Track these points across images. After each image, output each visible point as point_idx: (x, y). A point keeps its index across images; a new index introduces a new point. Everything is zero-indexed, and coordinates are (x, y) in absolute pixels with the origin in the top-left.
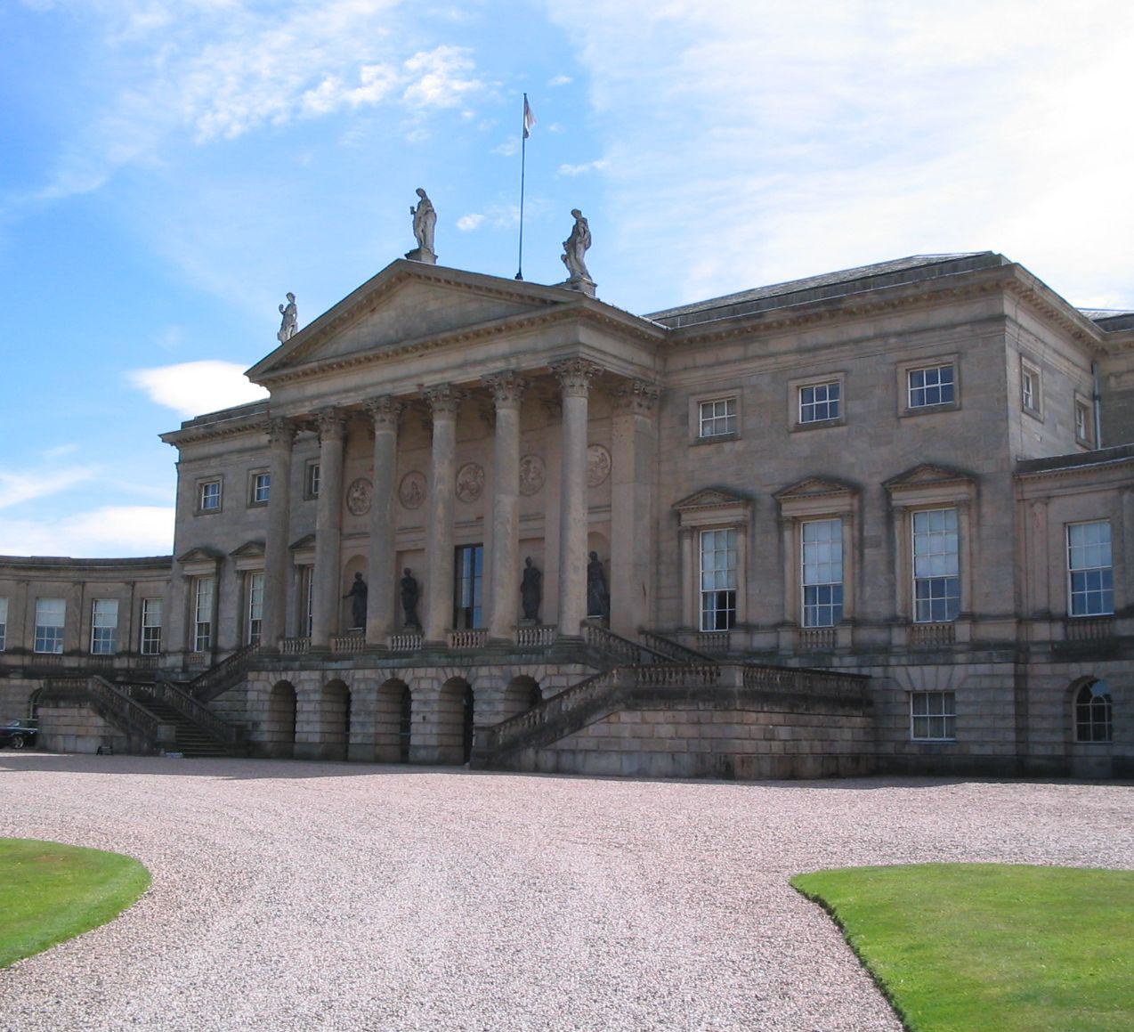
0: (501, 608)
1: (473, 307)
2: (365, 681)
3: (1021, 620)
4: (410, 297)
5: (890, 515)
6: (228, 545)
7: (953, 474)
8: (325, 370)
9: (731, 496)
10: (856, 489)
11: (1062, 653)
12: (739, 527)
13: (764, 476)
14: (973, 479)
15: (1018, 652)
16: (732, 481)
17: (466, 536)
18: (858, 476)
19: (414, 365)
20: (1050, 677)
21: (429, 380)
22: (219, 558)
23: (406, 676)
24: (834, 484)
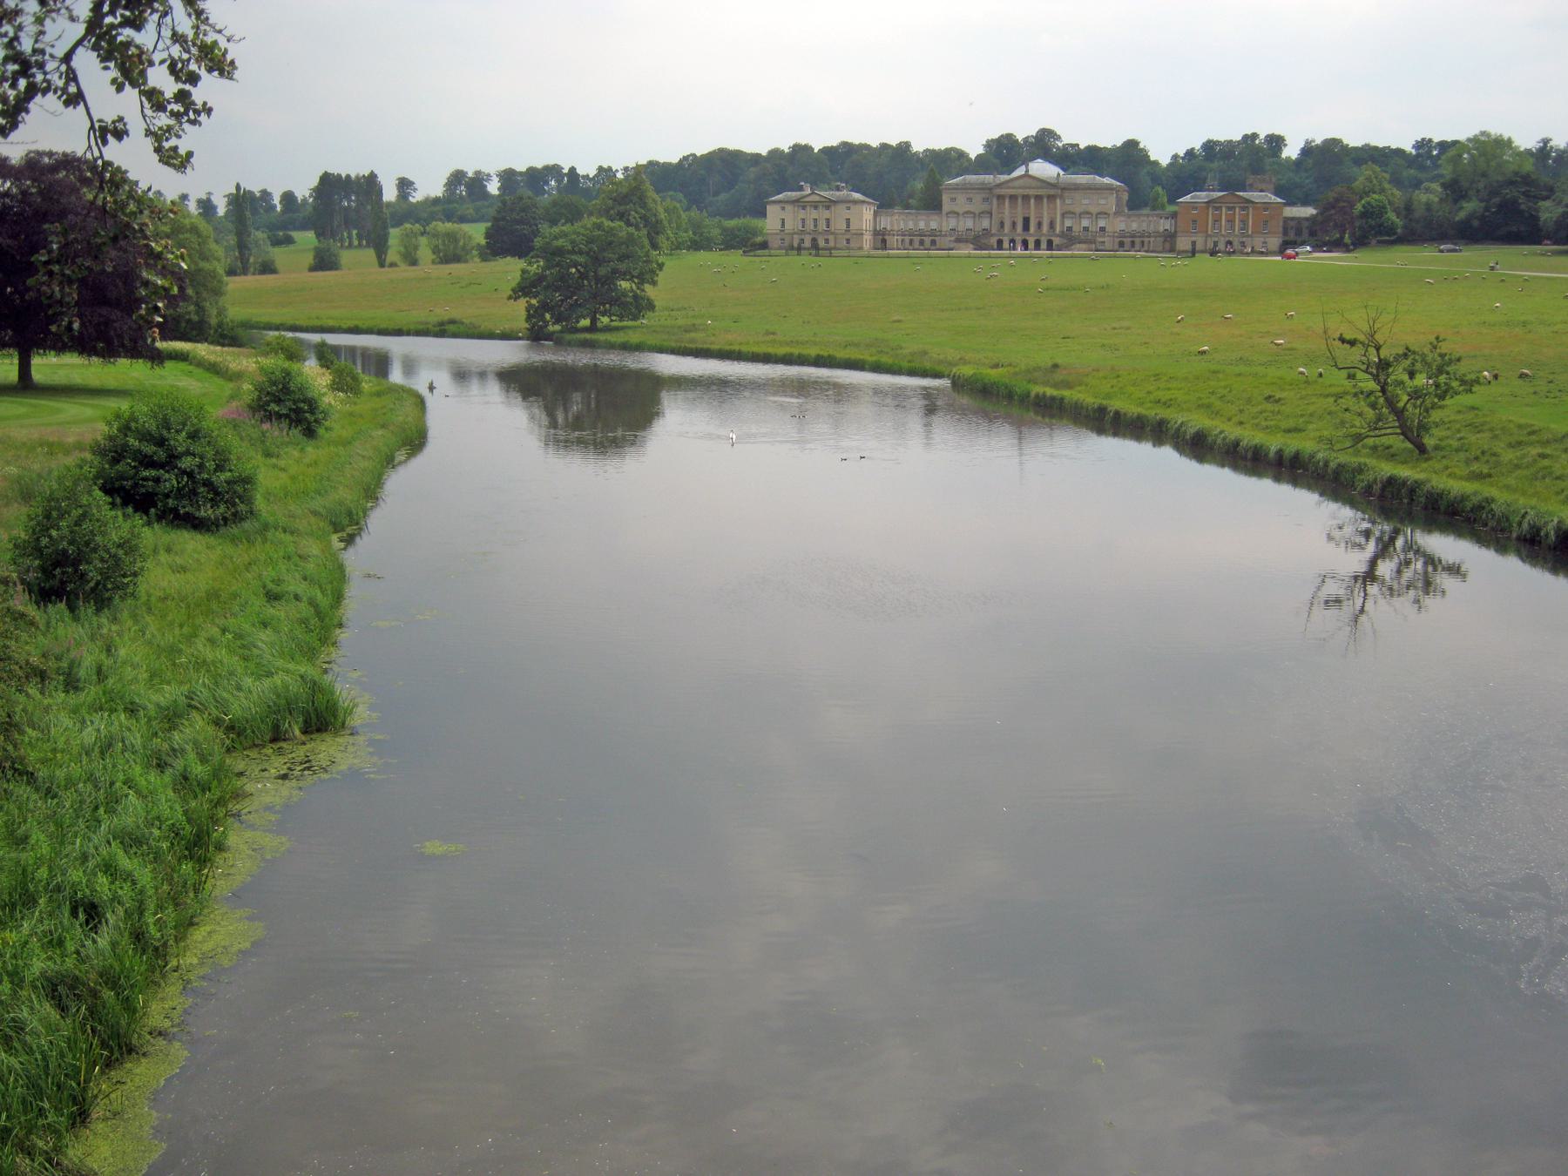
0: (1045, 228)
1: (1039, 184)
2: (1019, 239)
3: (1114, 233)
4: (1026, 179)
5: (1097, 218)
6: (961, 212)
7: (1106, 214)
8: (1009, 188)
9: (1073, 213)
10: (1092, 215)
11: (1117, 237)
12: (1072, 218)
13: (1078, 210)
14: (1109, 215)
15: (1114, 236)
16: (1072, 210)
17: (1027, 215)
18: (1092, 212)
19: (1028, 190)
20: (1118, 240)
21: (1031, 193)
22: (958, 214)
23: (1028, 238)
24: (1088, 213)
